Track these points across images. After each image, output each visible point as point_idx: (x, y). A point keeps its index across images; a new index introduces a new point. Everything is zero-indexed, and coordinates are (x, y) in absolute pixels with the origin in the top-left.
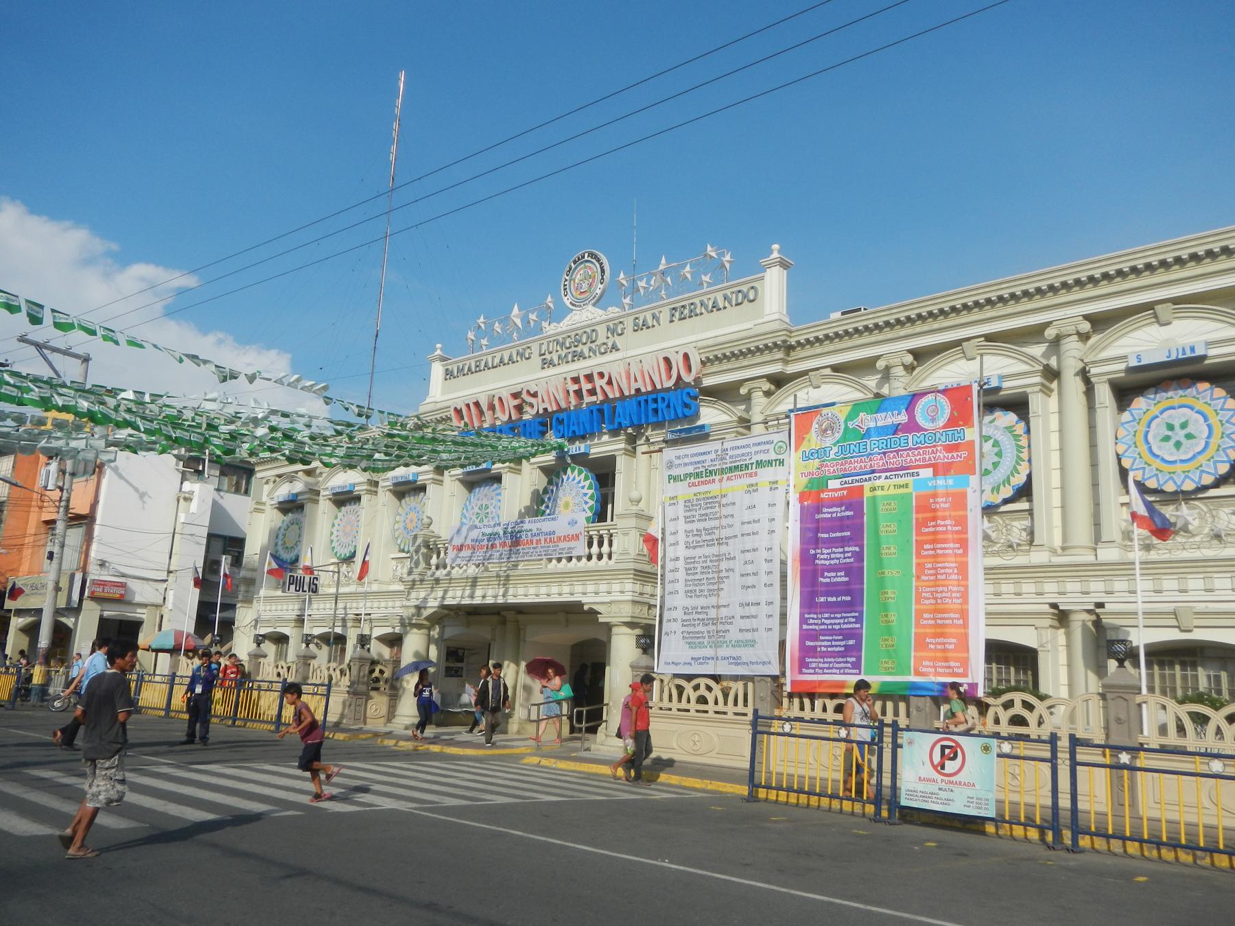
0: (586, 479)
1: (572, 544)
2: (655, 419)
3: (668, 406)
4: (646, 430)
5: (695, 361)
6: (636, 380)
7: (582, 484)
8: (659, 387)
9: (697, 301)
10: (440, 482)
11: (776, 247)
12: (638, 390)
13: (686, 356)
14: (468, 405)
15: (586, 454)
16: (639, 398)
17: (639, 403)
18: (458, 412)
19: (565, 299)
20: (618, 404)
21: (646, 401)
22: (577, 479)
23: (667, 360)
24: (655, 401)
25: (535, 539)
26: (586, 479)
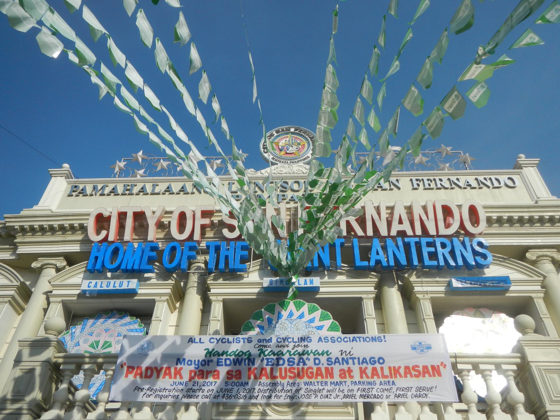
0: (323, 318)
1: (427, 381)
2: (435, 263)
3: (452, 253)
4: (410, 275)
5: (483, 215)
6: (401, 222)
7: (317, 323)
8: (432, 231)
9: (445, 179)
10: (19, 309)
11: (522, 155)
12: (402, 234)
13: (473, 210)
14: (122, 216)
15: (316, 290)
16: (406, 240)
17: (407, 246)
18: (102, 221)
19: (266, 155)
20: (376, 244)
21: (418, 245)
22: (307, 317)
23: (447, 211)
24: (429, 244)
25: (337, 368)
26: (323, 318)
